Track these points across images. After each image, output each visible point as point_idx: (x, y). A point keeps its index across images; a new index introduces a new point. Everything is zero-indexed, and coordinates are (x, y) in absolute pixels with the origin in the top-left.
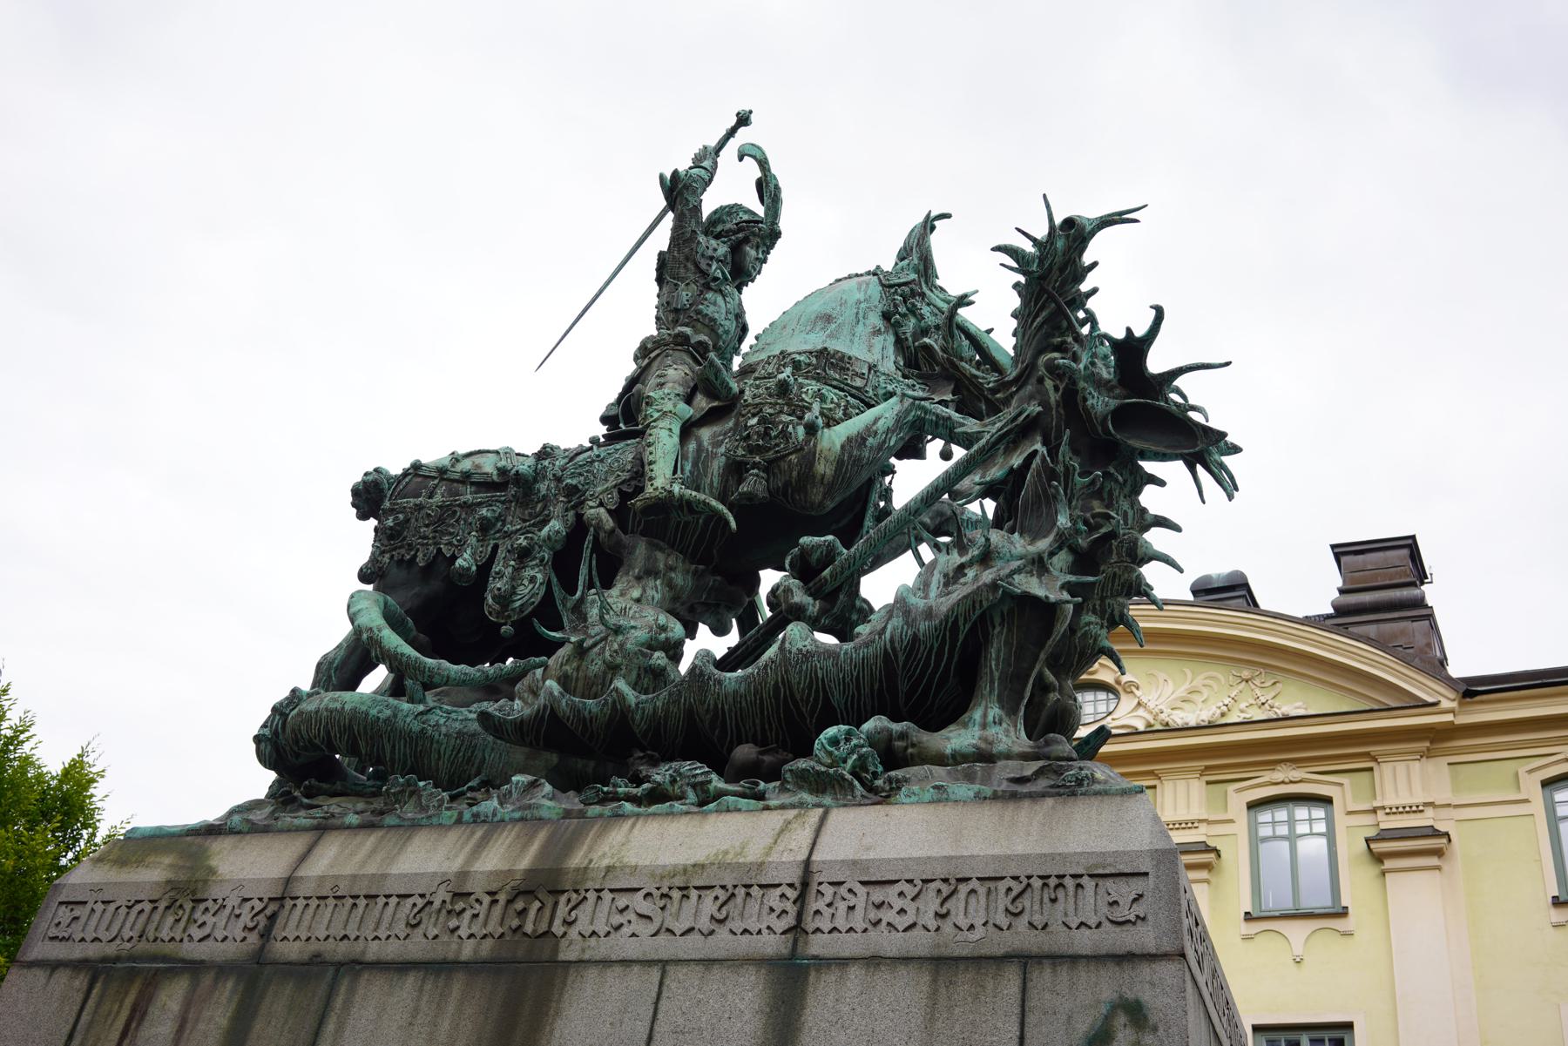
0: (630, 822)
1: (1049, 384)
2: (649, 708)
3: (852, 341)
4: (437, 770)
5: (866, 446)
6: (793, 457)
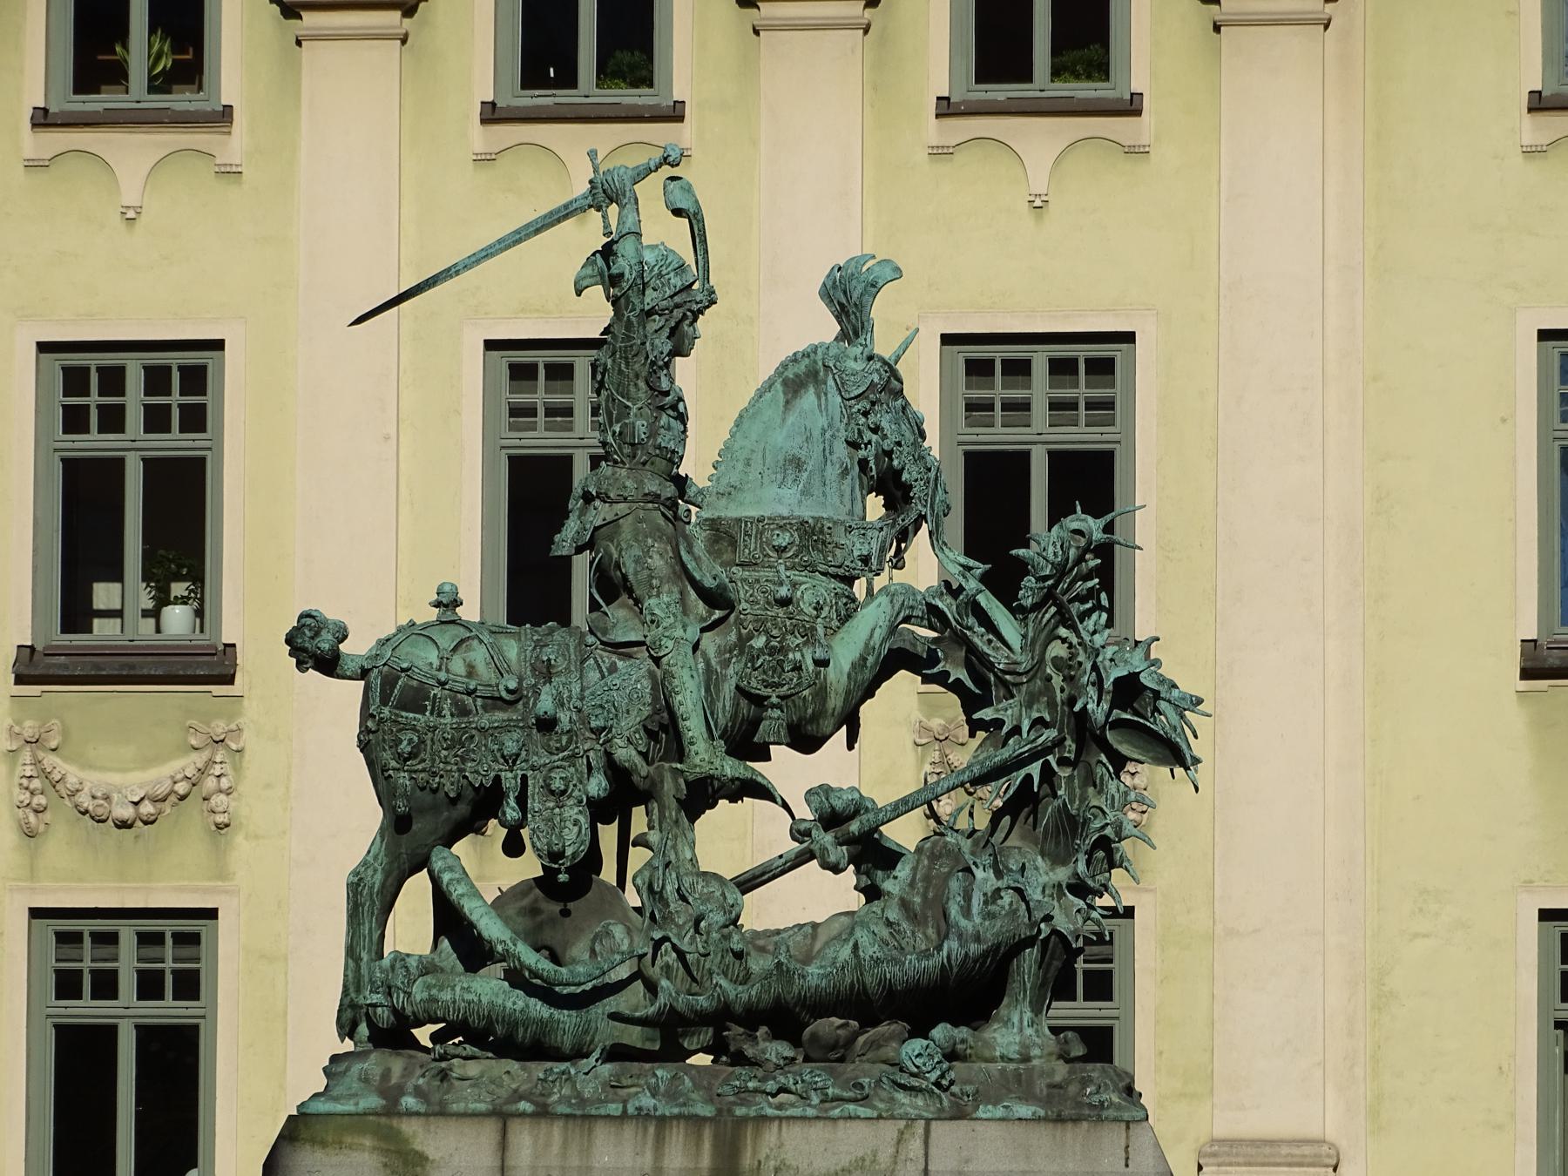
0: (776, 1123)
1: (1057, 681)
2: (745, 997)
3: (824, 494)
4: (562, 1043)
5: (867, 667)
6: (806, 693)
